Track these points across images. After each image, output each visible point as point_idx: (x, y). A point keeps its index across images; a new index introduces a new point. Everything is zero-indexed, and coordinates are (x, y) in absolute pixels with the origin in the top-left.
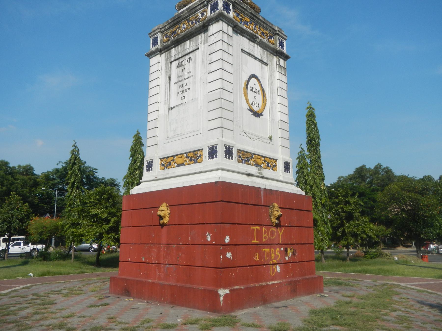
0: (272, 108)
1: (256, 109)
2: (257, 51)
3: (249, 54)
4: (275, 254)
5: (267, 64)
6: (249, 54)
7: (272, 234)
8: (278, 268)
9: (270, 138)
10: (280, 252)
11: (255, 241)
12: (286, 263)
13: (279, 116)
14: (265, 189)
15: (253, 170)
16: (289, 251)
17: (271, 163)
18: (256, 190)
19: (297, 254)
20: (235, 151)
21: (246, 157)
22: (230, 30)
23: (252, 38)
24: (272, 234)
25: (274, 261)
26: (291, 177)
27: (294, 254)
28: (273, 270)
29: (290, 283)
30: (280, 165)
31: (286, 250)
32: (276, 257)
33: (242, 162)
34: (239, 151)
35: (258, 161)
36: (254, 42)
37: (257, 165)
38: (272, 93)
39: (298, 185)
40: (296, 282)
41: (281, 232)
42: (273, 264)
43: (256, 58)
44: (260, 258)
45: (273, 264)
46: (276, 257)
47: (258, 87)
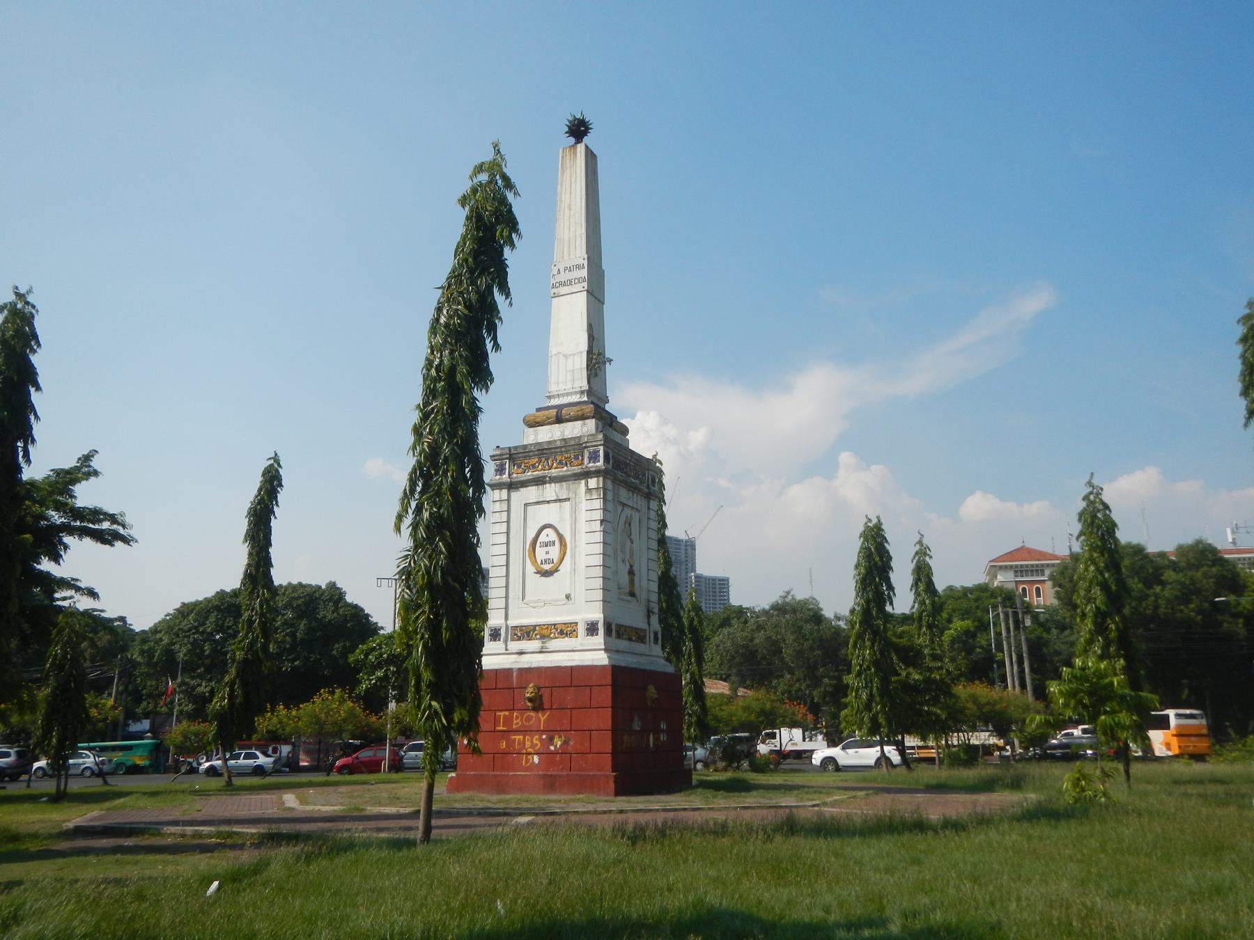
0: (573, 556)
1: (547, 567)
2: (550, 491)
3: (538, 503)
4: (535, 741)
6: (538, 503)
7: (529, 719)
8: (536, 759)
9: (568, 597)
10: (541, 740)
11: (501, 728)
12: (552, 753)
13: (583, 561)
14: (520, 670)
15: (535, 645)
17: (567, 630)
18: (508, 672)
20: (503, 632)
21: (526, 633)
22: (505, 492)
23: (539, 481)
25: (530, 750)
26: (599, 640)
27: (565, 743)
28: (527, 761)
29: (544, 776)
30: (581, 629)
31: (551, 740)
32: (533, 746)
35: (545, 632)
36: (544, 483)
37: (543, 637)
38: (574, 534)
39: (606, 650)
40: (555, 776)
43: (548, 502)
46: (533, 746)
47: (553, 536)
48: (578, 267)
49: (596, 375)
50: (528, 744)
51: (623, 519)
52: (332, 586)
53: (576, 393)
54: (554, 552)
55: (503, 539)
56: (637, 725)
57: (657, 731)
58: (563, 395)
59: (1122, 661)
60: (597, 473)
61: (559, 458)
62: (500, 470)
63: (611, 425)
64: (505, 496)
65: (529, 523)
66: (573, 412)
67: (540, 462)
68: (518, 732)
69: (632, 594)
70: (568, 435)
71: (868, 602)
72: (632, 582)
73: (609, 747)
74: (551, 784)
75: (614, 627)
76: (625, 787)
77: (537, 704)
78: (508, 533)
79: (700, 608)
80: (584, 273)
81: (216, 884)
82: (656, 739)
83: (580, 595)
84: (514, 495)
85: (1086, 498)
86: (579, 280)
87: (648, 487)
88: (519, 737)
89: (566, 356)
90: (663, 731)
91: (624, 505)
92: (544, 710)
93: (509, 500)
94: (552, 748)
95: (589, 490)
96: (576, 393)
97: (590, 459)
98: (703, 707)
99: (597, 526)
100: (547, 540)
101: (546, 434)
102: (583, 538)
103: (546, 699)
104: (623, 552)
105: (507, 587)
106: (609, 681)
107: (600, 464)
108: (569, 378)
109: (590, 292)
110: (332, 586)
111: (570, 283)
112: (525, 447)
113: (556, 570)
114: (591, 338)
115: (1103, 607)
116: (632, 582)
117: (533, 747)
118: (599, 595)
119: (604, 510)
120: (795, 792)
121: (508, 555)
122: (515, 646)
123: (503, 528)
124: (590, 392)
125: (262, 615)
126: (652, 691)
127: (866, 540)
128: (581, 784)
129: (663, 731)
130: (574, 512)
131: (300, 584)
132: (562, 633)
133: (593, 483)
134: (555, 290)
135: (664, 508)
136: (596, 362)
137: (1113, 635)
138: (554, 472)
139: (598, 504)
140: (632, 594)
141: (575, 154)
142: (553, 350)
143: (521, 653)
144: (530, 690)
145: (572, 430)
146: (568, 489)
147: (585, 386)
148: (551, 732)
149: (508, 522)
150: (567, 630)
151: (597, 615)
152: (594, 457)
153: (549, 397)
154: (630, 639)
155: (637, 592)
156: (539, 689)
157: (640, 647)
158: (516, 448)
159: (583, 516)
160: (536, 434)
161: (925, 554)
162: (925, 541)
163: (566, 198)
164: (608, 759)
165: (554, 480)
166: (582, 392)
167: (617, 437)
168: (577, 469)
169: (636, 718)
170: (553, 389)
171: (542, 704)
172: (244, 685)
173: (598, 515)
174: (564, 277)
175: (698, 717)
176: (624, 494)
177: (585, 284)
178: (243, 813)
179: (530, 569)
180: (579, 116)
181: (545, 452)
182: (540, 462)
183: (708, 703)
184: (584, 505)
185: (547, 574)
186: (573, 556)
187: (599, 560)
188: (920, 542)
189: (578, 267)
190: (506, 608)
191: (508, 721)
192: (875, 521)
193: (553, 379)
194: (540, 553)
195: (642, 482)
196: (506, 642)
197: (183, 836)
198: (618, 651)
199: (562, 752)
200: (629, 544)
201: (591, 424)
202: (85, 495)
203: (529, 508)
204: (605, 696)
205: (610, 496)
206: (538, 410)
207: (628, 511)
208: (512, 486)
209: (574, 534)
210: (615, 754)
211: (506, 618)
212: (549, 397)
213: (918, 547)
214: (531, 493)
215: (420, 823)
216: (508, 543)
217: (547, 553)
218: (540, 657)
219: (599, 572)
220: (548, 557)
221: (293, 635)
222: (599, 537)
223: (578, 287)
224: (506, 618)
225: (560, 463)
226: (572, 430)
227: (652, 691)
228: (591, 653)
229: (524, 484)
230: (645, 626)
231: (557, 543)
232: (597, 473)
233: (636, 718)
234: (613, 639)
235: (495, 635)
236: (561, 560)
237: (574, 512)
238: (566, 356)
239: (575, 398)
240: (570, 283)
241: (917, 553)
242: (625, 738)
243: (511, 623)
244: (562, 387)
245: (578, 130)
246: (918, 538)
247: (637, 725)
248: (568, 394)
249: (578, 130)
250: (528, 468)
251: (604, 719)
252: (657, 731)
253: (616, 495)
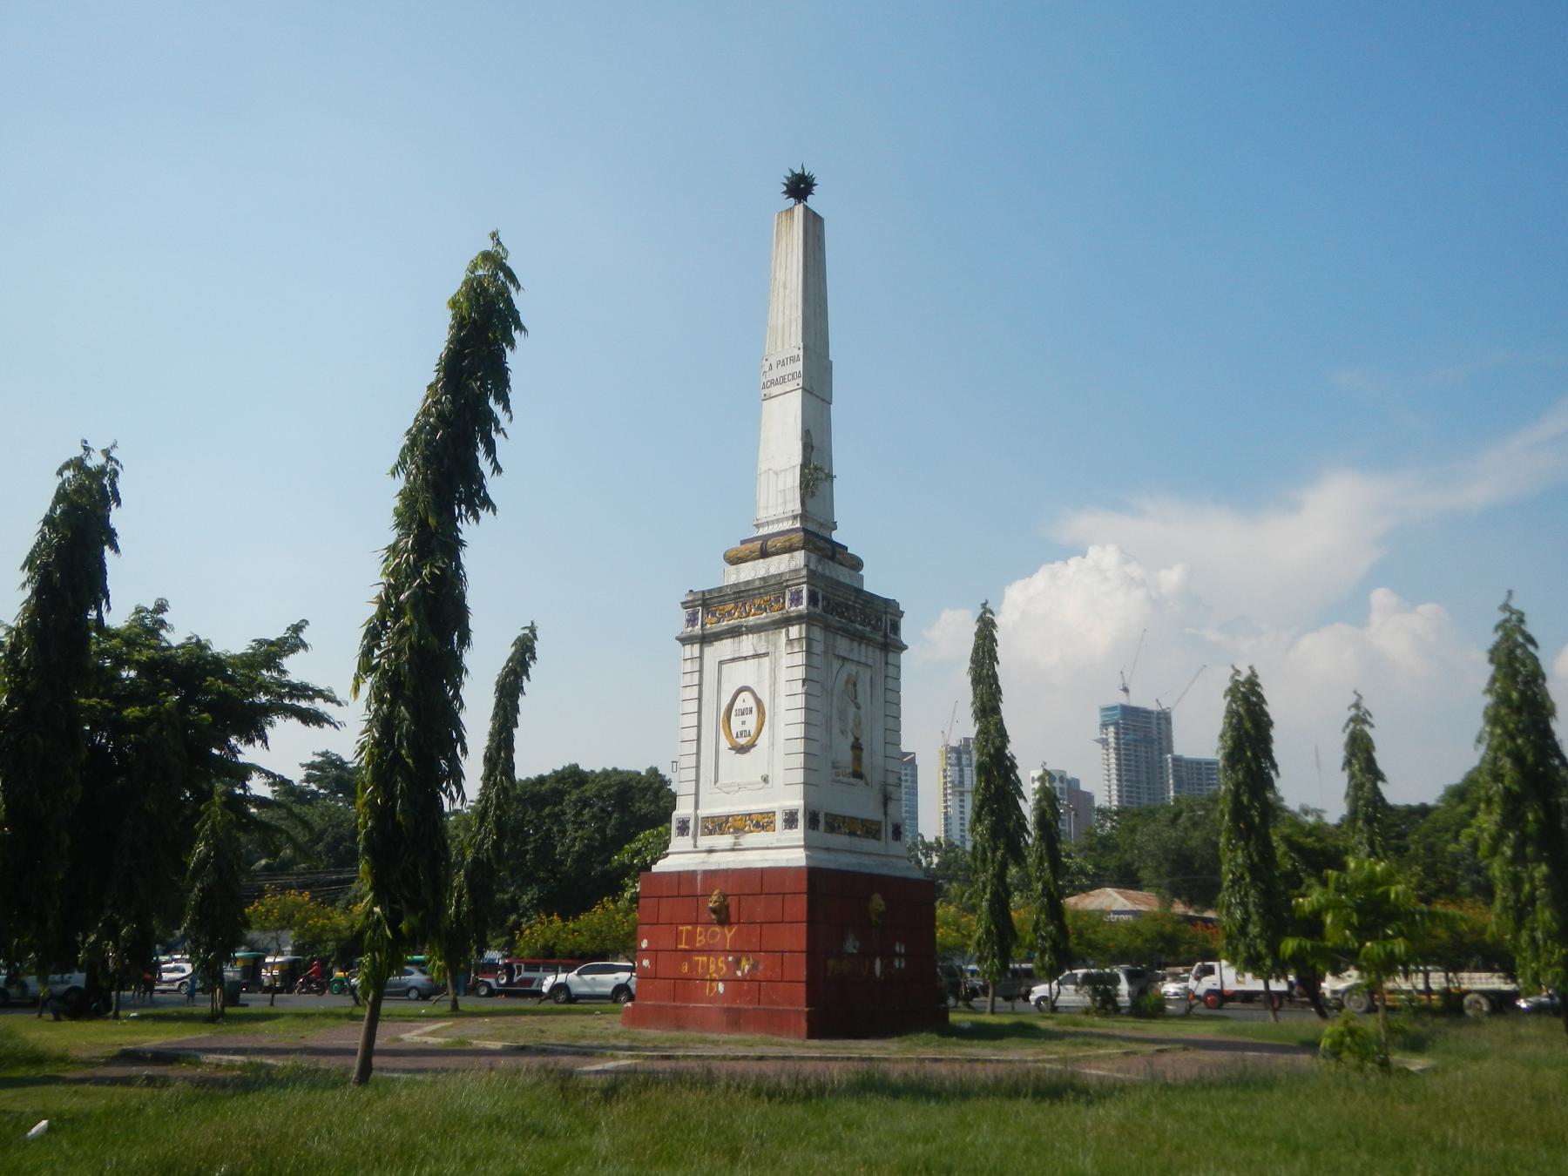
1: (743, 741)
2: (748, 644)
3: (733, 660)
4: (717, 965)
5: (766, 654)
6: (733, 660)
7: (714, 935)
8: (721, 987)
9: (765, 780)
10: (727, 963)
12: (739, 980)
14: (705, 872)
15: (725, 840)
16: (744, 962)
17: (762, 822)
19: (761, 967)
20: (691, 824)
21: (717, 825)
22: (697, 647)
23: (735, 632)
24: (714, 935)
26: (798, 834)
27: (754, 967)
28: (711, 989)
29: (727, 1010)
30: (779, 821)
31: (738, 962)
32: (718, 970)
33: (710, 833)
34: (705, 819)
35: (738, 824)
36: (741, 634)
38: (773, 699)
40: (738, 1010)
41: (730, 933)
42: (713, 980)
44: (691, 969)
45: (713, 980)
46: (718, 970)
47: (751, 703)
48: (793, 359)
49: (813, 494)
50: (712, 967)
51: (843, 676)
52: (653, 772)
53: (787, 519)
54: (751, 722)
55: (693, 706)
56: (851, 946)
57: (888, 956)
58: (773, 522)
59: (1544, 868)
60: (799, 619)
61: (757, 602)
62: (692, 621)
63: (832, 558)
64: (696, 653)
65: (724, 686)
66: (778, 543)
67: (736, 608)
68: (700, 951)
69: (858, 775)
70: (773, 571)
71: (1238, 785)
72: (858, 759)
73: (802, 974)
74: (735, 1020)
75: (822, 819)
76: (820, 1027)
77: (723, 916)
78: (700, 699)
79: (1055, 798)
80: (799, 366)
81: (44, 1123)
82: (886, 967)
83: (778, 776)
84: (708, 650)
85: (1500, 626)
86: (794, 376)
87: (886, 636)
88: (702, 959)
89: (776, 473)
90: (900, 955)
91: (844, 659)
92: (730, 924)
93: (701, 658)
94: (739, 973)
95: (790, 642)
96: (787, 519)
97: (792, 601)
98: (1062, 928)
99: (798, 687)
101: (751, 571)
102: (783, 702)
103: (733, 910)
104: (843, 719)
105: (698, 767)
106: (804, 888)
107: (803, 607)
108: (780, 500)
109: (807, 390)
110: (653, 772)
111: (783, 380)
112: (720, 589)
113: (753, 745)
114: (808, 447)
115: (1516, 788)
116: (858, 759)
117: (719, 971)
118: (799, 776)
119: (809, 665)
120: (1067, 1040)
121: (699, 727)
122: (705, 842)
123: (694, 692)
124: (804, 516)
125: (498, 807)
126: (877, 903)
127: (1233, 700)
128: (772, 1022)
129: (900, 955)
130: (773, 670)
131: (615, 770)
132: (757, 825)
133: (795, 631)
134: (766, 391)
135: (997, 669)
136: (815, 476)
137: (1532, 828)
138: (751, 620)
139: (800, 658)
140: (858, 775)
141: (792, 218)
142: (763, 466)
143: (710, 851)
144: (714, 898)
145: (779, 565)
146: (767, 641)
147: (796, 507)
148: (738, 953)
149: (700, 685)
150: (762, 822)
151: (796, 802)
152: (796, 600)
153: (758, 526)
154: (852, 834)
155: (865, 770)
156: (725, 896)
157: (869, 844)
158: (710, 591)
159: (783, 675)
160: (738, 572)
161: (1365, 721)
162: (1365, 704)
163: (780, 275)
164: (801, 989)
165: (752, 630)
166: (795, 517)
167: (843, 575)
168: (776, 615)
169: (851, 937)
170: (763, 515)
171: (728, 916)
172: (472, 891)
173: (800, 673)
174: (776, 373)
175: (1054, 941)
176: (843, 645)
177: (800, 381)
178: (265, 1042)
179: (725, 744)
180: (798, 171)
181: (742, 595)
182: (736, 608)
183: (1068, 920)
184: (785, 660)
185: (742, 750)
186: (772, 727)
187: (799, 731)
188: (1357, 706)
189: (793, 359)
190: (697, 794)
191: (691, 937)
192: (1245, 673)
193: (762, 504)
194: (736, 723)
195: (874, 628)
196: (695, 837)
197: (218, 1066)
198: (828, 849)
199: (750, 979)
200: (853, 709)
201: (799, 558)
202: (296, 668)
203: (725, 667)
204: (799, 907)
205: (818, 648)
206: (743, 542)
207: (852, 668)
208: (705, 639)
209: (773, 699)
210: (812, 983)
211: (697, 807)
212: (758, 526)
213: (1353, 712)
214: (725, 648)
215: (356, 1062)
216: (699, 712)
218: (731, 856)
219: (800, 746)
221: (601, 830)
222: (800, 701)
223: (791, 385)
224: (697, 807)
225: (759, 608)
226: (779, 565)
227: (877, 903)
228: (786, 850)
229: (718, 636)
230: (879, 816)
231: (755, 710)
232: (799, 619)
233: (851, 937)
234: (821, 835)
235: (683, 828)
236: (759, 731)
237: (774, 670)
238: (776, 473)
239: (787, 525)
240: (783, 380)
241: (1352, 720)
242: (831, 963)
243: (703, 812)
244: (771, 512)
245: (800, 187)
246: (1354, 699)
247: (851, 946)
248: (778, 521)
249: (800, 187)
250: (723, 616)
251: (795, 938)
252: (888, 956)
253: (829, 651)
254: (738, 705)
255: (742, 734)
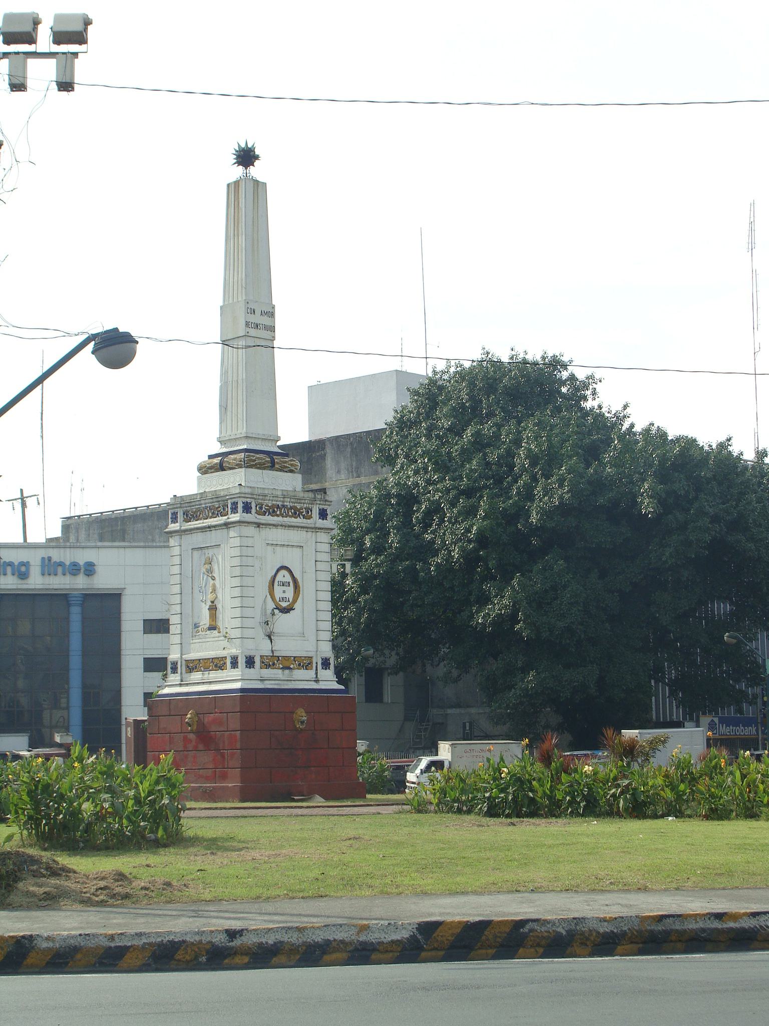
1: (284, 604)
17: (305, 663)
47: (288, 578)
54: (290, 592)
100: (284, 580)
126: (301, 714)
132: (300, 666)
180: (243, 145)
185: (287, 610)
194: (278, 592)
208: (258, 525)
217: (284, 592)
220: (284, 595)
227: (301, 714)
231: (291, 584)
236: (295, 600)
254: (279, 577)
255: (283, 599)
